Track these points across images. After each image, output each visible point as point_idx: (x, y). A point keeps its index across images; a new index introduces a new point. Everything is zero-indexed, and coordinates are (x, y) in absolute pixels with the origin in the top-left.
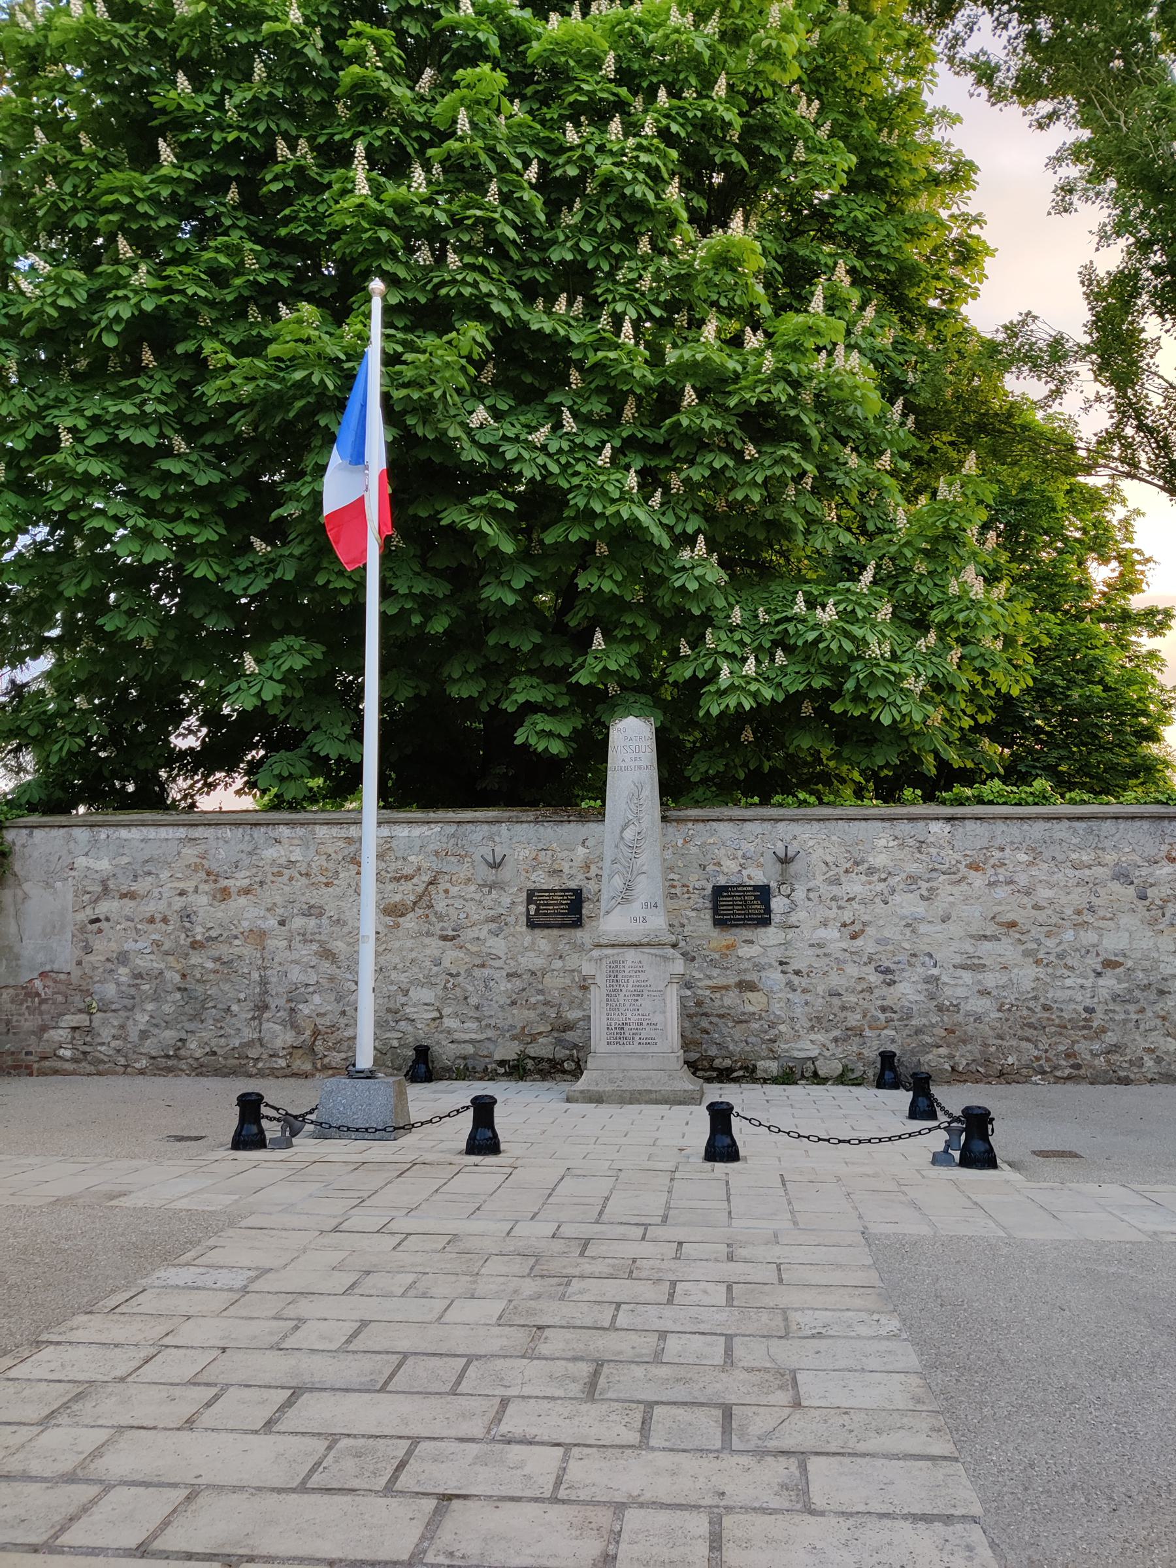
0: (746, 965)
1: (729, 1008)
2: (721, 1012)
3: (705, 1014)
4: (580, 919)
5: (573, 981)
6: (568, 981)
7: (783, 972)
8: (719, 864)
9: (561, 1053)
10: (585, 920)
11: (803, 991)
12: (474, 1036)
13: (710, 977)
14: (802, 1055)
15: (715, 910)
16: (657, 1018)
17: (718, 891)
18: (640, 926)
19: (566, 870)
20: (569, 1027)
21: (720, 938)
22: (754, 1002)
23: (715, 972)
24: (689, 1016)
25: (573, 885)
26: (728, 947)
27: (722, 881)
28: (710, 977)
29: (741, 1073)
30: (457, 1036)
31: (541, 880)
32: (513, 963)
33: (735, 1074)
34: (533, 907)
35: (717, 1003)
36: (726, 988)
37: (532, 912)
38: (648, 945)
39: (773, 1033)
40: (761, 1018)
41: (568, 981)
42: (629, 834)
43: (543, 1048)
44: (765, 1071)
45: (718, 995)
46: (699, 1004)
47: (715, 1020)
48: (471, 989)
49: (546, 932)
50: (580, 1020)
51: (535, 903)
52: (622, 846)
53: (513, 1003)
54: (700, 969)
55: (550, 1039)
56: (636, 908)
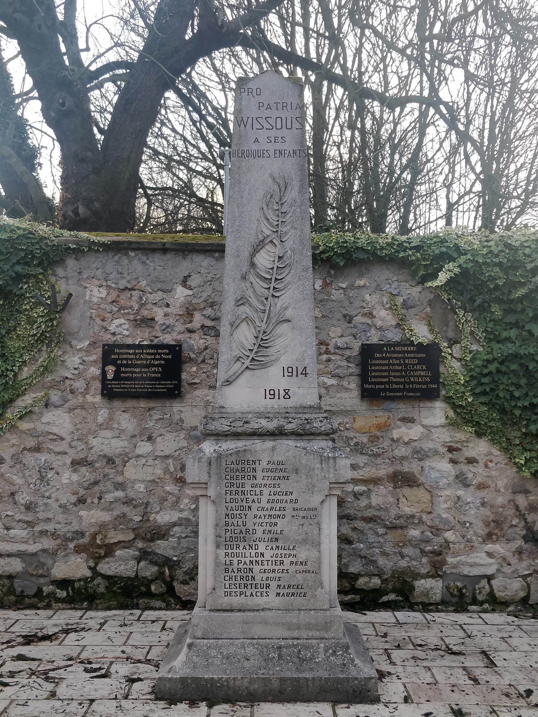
0: (401, 451)
1: (380, 509)
4: (178, 387)
5: (166, 471)
6: (159, 472)
7: (453, 461)
8: (370, 315)
9: (148, 571)
10: (185, 387)
11: (481, 487)
12: (23, 547)
15: (364, 377)
17: (368, 352)
19: (159, 318)
20: (160, 533)
21: (367, 417)
22: (411, 502)
23: (361, 460)
25: (168, 339)
26: (379, 427)
27: (374, 338)
29: (392, 597)
31: (121, 329)
32: (81, 446)
33: (385, 599)
34: (111, 370)
36: (376, 481)
37: (110, 376)
40: (421, 522)
41: (159, 472)
43: (121, 565)
47: (359, 524)
48: (18, 480)
49: (130, 403)
50: (174, 525)
51: (113, 363)
52: (252, 278)
53: (81, 501)
55: (132, 552)
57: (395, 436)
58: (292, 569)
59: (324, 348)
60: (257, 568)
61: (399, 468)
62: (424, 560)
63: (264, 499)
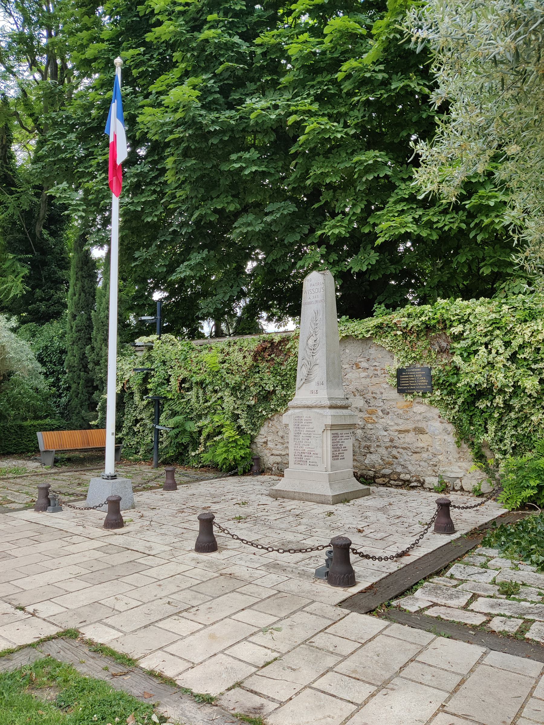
0: (419, 417)
2: (404, 446)
3: (395, 447)
12: (281, 452)
13: (397, 424)
14: (453, 475)
15: (398, 384)
16: (318, 451)
18: (314, 396)
22: (423, 441)
23: (400, 421)
24: (387, 448)
28: (397, 424)
30: (275, 452)
35: (402, 440)
36: (408, 431)
38: (315, 407)
39: (435, 459)
42: (311, 342)
44: (430, 484)
45: (403, 435)
46: (392, 441)
48: (279, 427)
54: (392, 420)
56: (313, 385)
57: (415, 411)
58: (314, 456)
59: (383, 371)
60: (303, 455)
61: (417, 425)
62: (429, 468)
63: (305, 430)
